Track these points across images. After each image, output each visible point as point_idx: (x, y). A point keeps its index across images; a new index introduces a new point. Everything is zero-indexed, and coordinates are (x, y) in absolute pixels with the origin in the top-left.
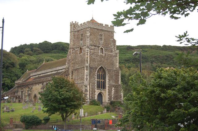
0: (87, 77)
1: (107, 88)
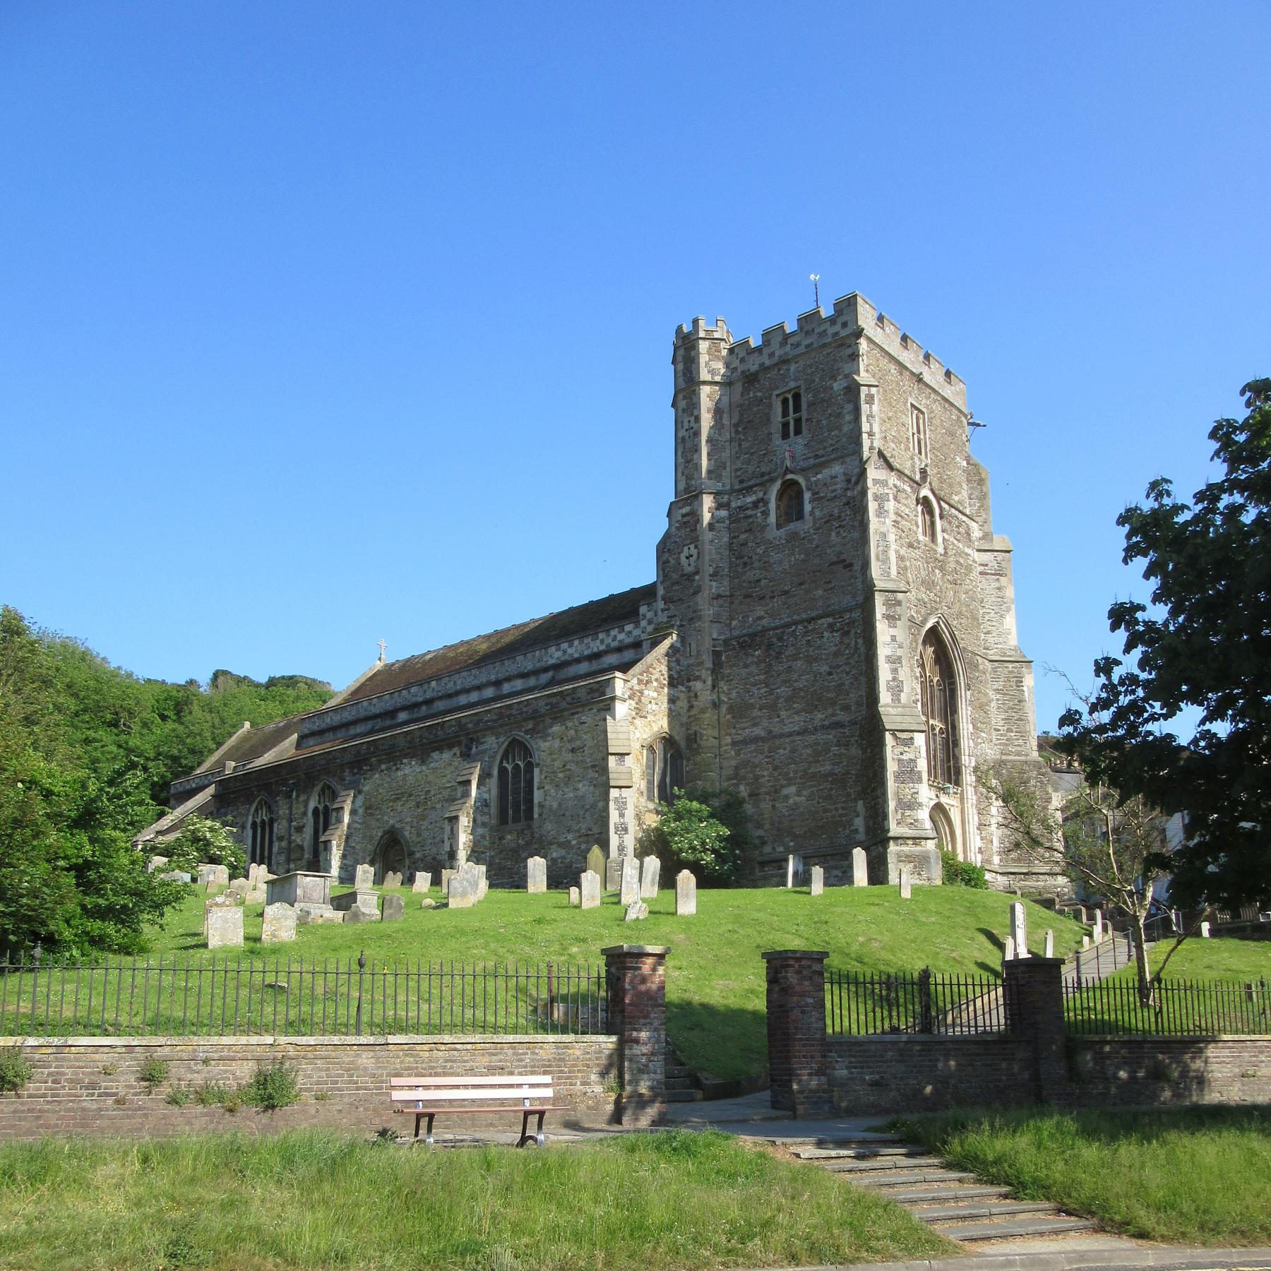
0: (895, 671)
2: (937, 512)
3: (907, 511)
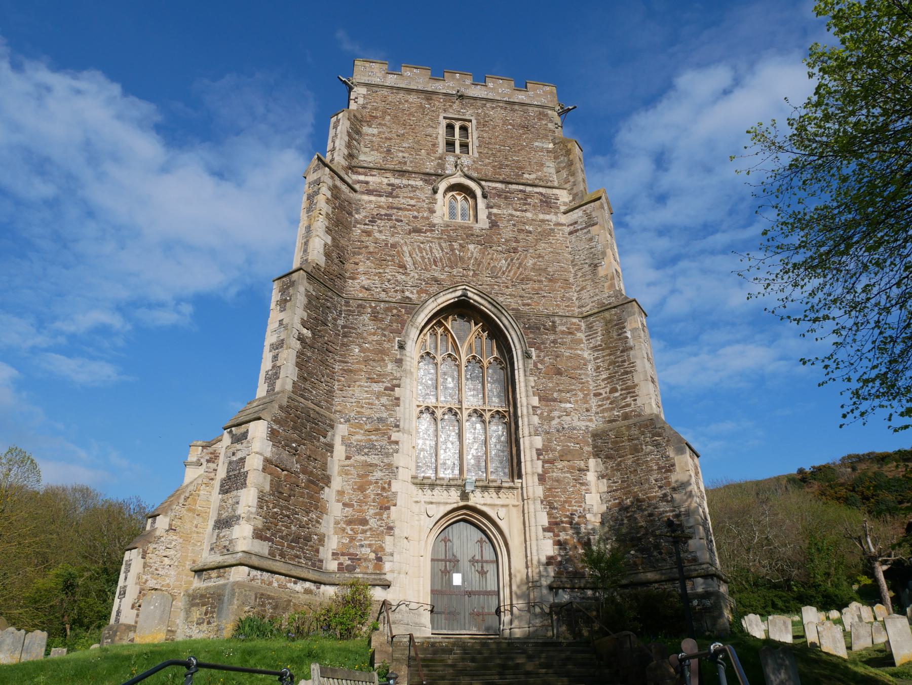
0: (275, 358)
1: (531, 465)
2: (479, 192)
3: (412, 202)
